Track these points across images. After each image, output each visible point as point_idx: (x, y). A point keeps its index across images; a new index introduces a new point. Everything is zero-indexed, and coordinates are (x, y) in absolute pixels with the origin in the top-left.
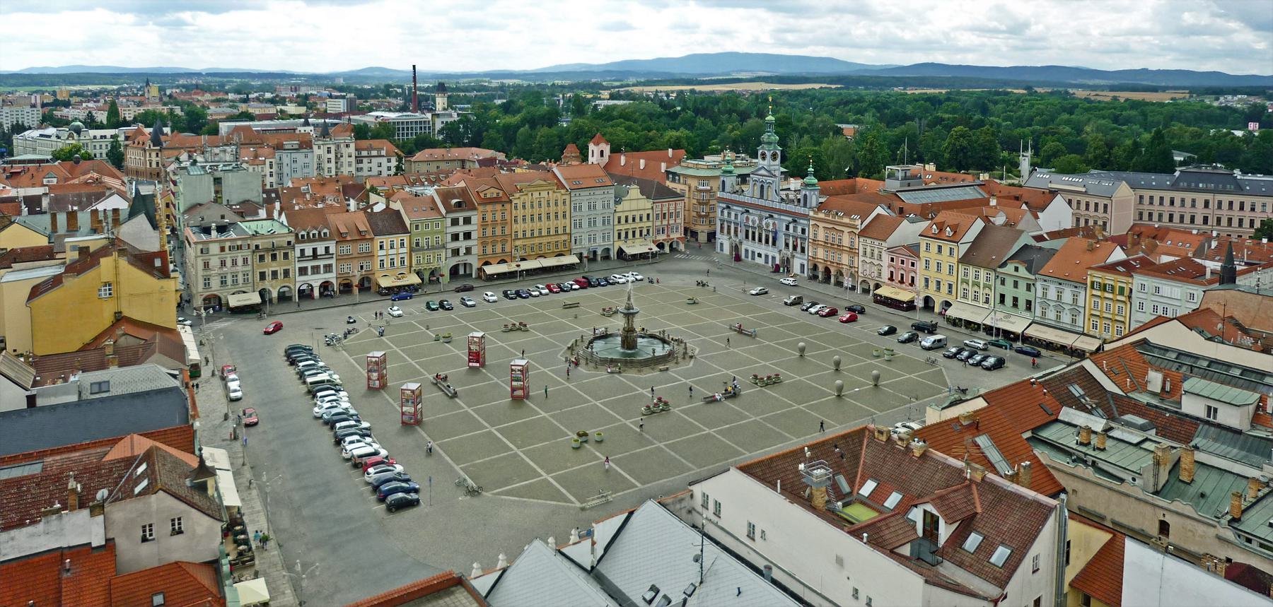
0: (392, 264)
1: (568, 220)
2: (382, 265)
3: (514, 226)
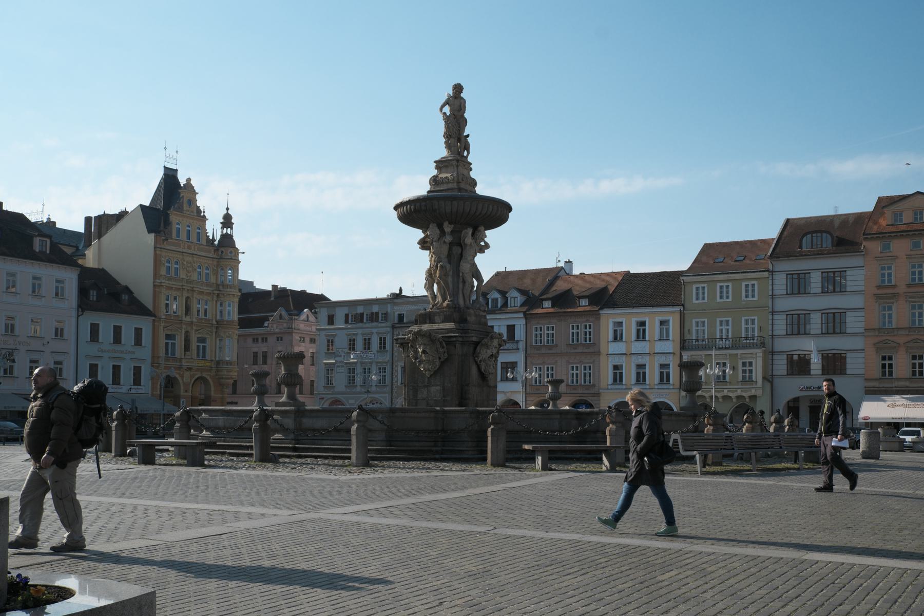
0: (641, 378)
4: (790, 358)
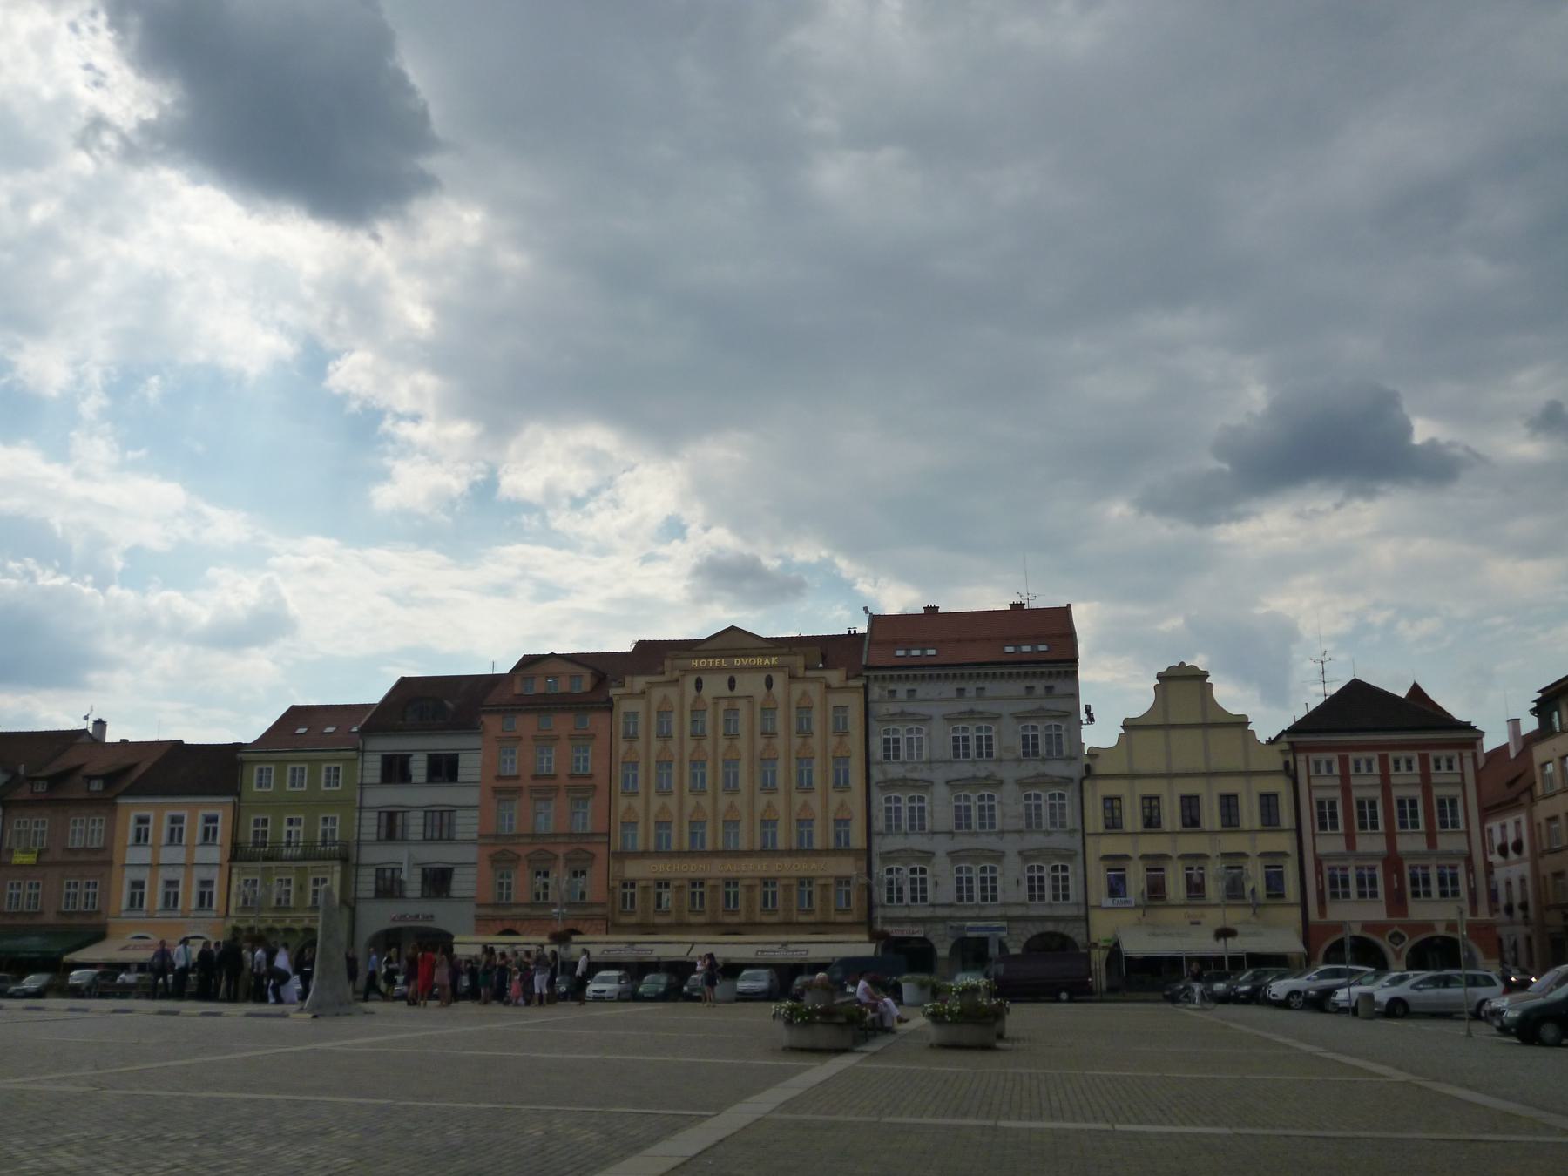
0: (171, 901)
1: (855, 799)
2: (136, 901)
3: (622, 803)
4: (380, 872)
